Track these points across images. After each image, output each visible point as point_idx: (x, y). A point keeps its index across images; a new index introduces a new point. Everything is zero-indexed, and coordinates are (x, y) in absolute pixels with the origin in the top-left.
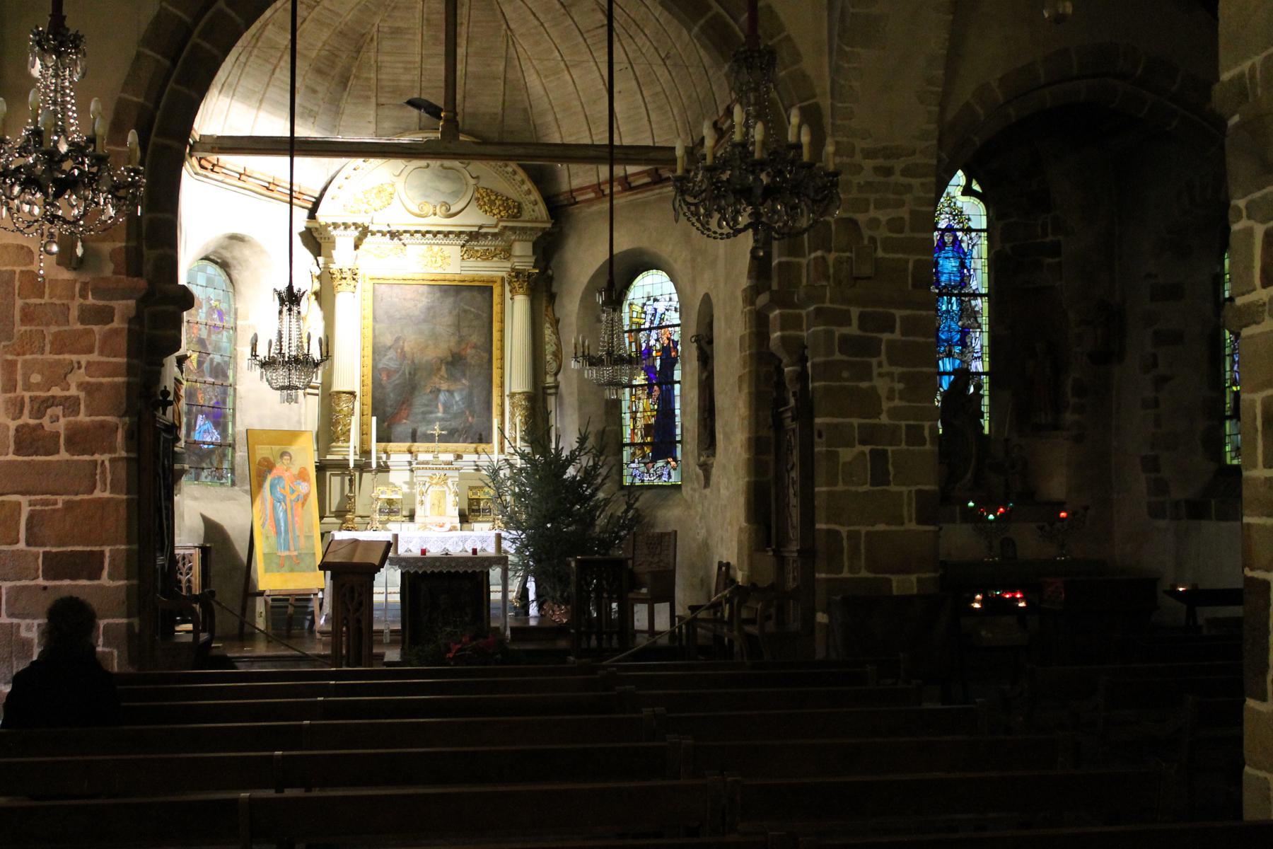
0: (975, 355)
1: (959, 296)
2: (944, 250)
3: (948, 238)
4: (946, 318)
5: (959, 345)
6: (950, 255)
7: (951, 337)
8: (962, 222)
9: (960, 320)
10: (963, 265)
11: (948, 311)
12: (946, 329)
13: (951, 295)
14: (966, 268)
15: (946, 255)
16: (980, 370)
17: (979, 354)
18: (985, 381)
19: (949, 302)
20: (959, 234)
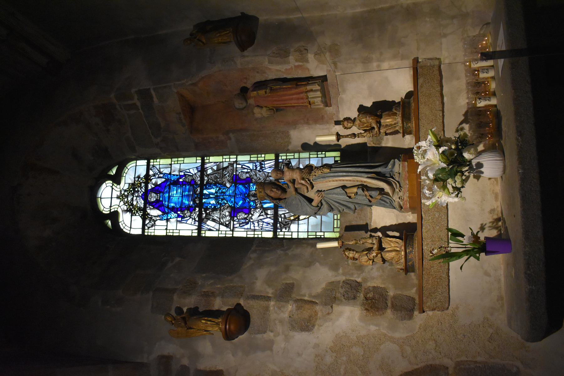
0: (258, 168)
1: (203, 186)
2: (162, 201)
3: (153, 197)
4: (222, 200)
5: (249, 186)
6: (167, 195)
7: (241, 194)
8: (141, 184)
9: (225, 185)
10: (176, 183)
11: (216, 198)
12: (233, 199)
13: (202, 195)
14: (178, 179)
15: (167, 199)
16: (273, 163)
17: (258, 164)
18: (285, 158)
19: (208, 196)
20: (150, 186)
